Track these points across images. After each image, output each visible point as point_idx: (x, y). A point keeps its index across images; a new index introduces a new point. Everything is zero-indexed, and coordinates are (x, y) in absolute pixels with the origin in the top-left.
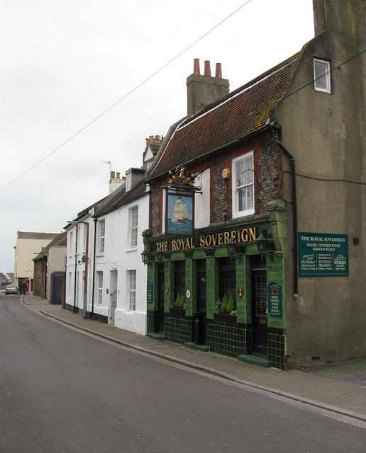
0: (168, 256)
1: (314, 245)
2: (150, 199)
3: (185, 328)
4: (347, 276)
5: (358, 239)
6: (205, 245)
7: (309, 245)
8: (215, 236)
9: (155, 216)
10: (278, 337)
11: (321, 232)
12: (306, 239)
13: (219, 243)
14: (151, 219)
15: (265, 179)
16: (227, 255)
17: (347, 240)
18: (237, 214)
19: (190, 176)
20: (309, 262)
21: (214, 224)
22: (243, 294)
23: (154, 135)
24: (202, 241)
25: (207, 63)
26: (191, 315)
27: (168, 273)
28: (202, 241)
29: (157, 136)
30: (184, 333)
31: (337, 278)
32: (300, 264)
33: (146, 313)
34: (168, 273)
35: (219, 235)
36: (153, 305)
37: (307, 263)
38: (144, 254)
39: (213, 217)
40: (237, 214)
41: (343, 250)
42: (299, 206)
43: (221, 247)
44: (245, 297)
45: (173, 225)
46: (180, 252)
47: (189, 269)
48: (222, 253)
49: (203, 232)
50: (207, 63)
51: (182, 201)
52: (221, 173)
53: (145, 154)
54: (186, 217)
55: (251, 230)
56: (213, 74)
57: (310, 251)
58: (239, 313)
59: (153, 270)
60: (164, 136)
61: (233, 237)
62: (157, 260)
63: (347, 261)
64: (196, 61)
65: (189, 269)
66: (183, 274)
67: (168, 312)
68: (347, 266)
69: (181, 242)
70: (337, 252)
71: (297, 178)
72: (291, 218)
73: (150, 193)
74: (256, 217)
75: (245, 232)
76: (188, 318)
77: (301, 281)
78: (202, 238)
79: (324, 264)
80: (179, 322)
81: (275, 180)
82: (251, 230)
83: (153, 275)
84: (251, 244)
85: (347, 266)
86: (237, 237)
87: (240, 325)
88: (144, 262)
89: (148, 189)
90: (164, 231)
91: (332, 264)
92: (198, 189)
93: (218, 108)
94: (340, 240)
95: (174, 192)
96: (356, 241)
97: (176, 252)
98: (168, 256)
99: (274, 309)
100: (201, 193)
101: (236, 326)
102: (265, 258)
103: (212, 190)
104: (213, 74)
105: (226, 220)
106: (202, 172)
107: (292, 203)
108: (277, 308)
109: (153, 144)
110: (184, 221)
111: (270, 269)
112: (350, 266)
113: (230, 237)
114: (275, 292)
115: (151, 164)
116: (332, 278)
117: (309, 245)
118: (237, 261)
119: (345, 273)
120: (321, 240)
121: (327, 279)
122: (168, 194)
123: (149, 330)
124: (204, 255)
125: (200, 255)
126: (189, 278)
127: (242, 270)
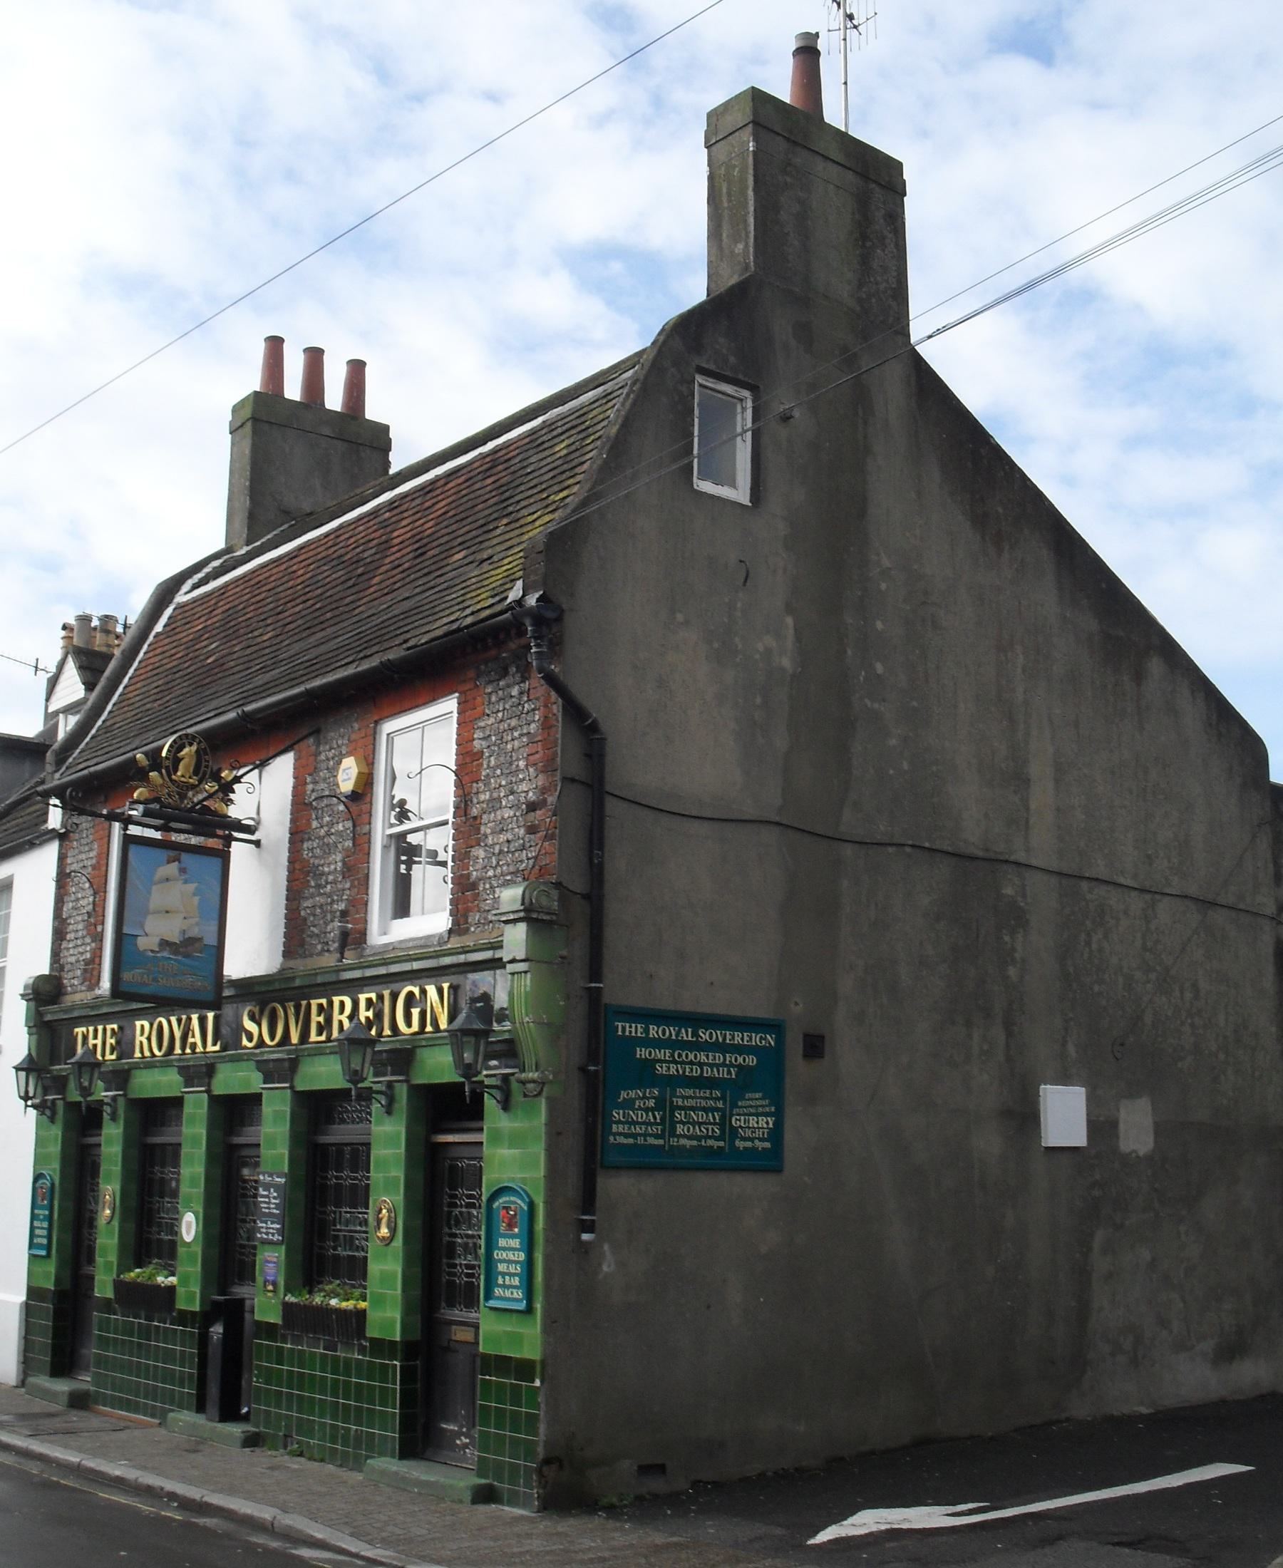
0: (120, 1077)
1: (660, 1054)
2: (62, 858)
3: (168, 1356)
4: (778, 1170)
5: (821, 1038)
6: (261, 1043)
7: (642, 1053)
8: (298, 1008)
9: (77, 926)
10: (516, 1390)
11: (687, 1006)
12: (635, 1030)
13: (314, 1037)
14: (59, 934)
15: (494, 804)
16: (340, 1083)
17: (780, 1041)
18: (387, 933)
19: (216, 777)
20: (641, 1116)
21: (300, 965)
22: (393, 1231)
23: (96, 612)
24: (249, 1025)
25: (315, 357)
26: (197, 1308)
27: (112, 1141)
28: (249, 1025)
29: (107, 619)
30: (168, 1377)
31: (739, 1178)
32: (608, 1121)
33: (22, 1297)
34: (112, 1141)
35: (314, 1003)
36: (51, 1267)
37: (632, 1120)
38: (29, 1067)
39: (296, 934)
40: (387, 933)
41: (767, 1077)
42: (614, 910)
43: (319, 1051)
44: (398, 1242)
45: (142, 959)
46: (165, 1064)
47: (194, 1131)
48: (325, 1073)
49: (250, 990)
50: (315, 357)
51: (183, 871)
52: (333, 771)
53: (53, 683)
54: (195, 932)
55: (431, 990)
56: (334, 399)
57: (645, 1074)
58: (379, 1301)
59: (56, 1131)
60: (131, 621)
61: (364, 1014)
62: (74, 1096)
63: (779, 1116)
64: (275, 345)
65: (194, 1131)
66: (172, 1154)
67: (110, 1294)
68: (776, 1135)
69: (170, 1024)
70: (744, 1082)
71: (611, 805)
72: (579, 950)
73: (62, 837)
74: (455, 943)
75: (411, 994)
76: (184, 1318)
77: (614, 1186)
78: (252, 1018)
79: (695, 1126)
80: (146, 1333)
81: (532, 807)
82: (431, 990)
83: (55, 1149)
84: (432, 1043)
85: (776, 1135)
86: (379, 1015)
87: (380, 1346)
88: (26, 1098)
89: (55, 818)
90: (106, 984)
91: (722, 1125)
92: (250, 830)
93: (340, 527)
94: (756, 1039)
95: (157, 835)
96: (814, 1046)
97: (150, 1064)
98: (120, 1077)
99: (504, 1286)
100: (257, 843)
101: (362, 1350)
102: (478, 1099)
103: (298, 834)
104: (334, 399)
105: (341, 951)
106: (262, 765)
107: (586, 897)
108: (516, 1281)
109: (91, 651)
110: (187, 946)
111: (496, 1137)
112: (789, 1137)
113: (354, 1015)
114: (510, 1226)
115: (73, 720)
116: (723, 1178)
117: (642, 1053)
118: (375, 1107)
119: (768, 1161)
120: (687, 1035)
121: (702, 1181)
122: (128, 841)
123: (27, 1363)
124: (252, 1080)
125: (236, 1079)
126: (192, 1171)
127: (388, 1138)
